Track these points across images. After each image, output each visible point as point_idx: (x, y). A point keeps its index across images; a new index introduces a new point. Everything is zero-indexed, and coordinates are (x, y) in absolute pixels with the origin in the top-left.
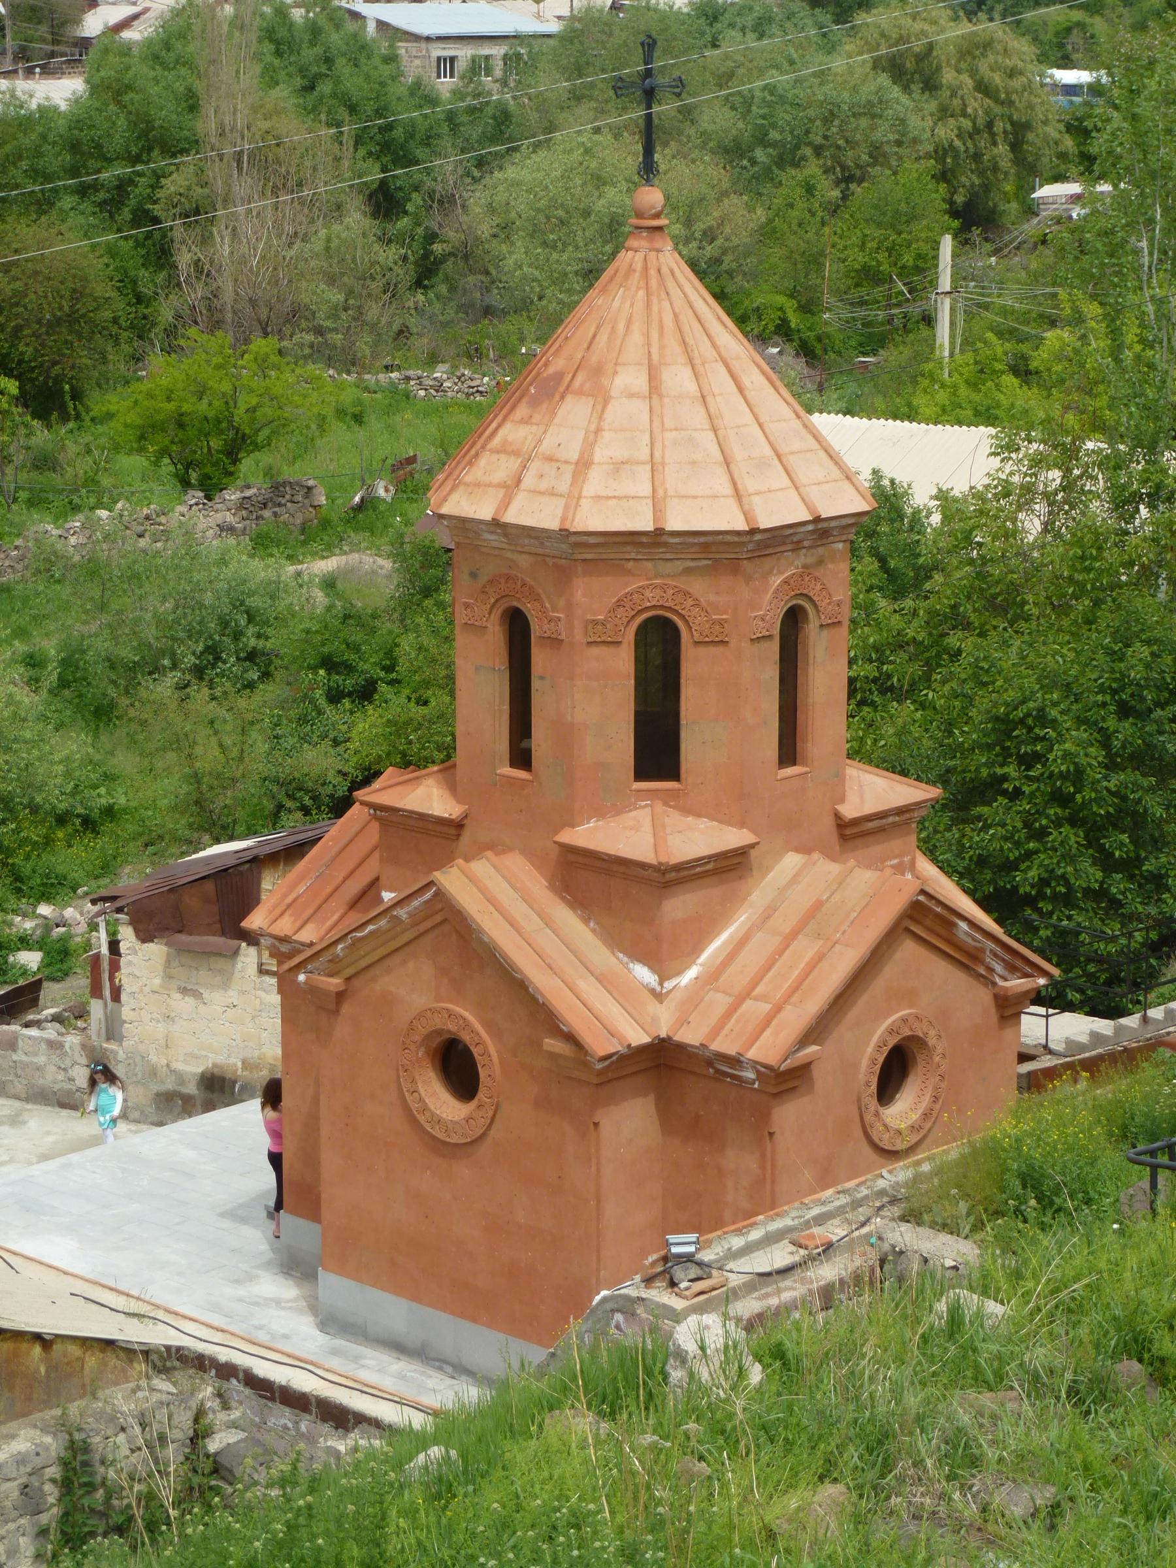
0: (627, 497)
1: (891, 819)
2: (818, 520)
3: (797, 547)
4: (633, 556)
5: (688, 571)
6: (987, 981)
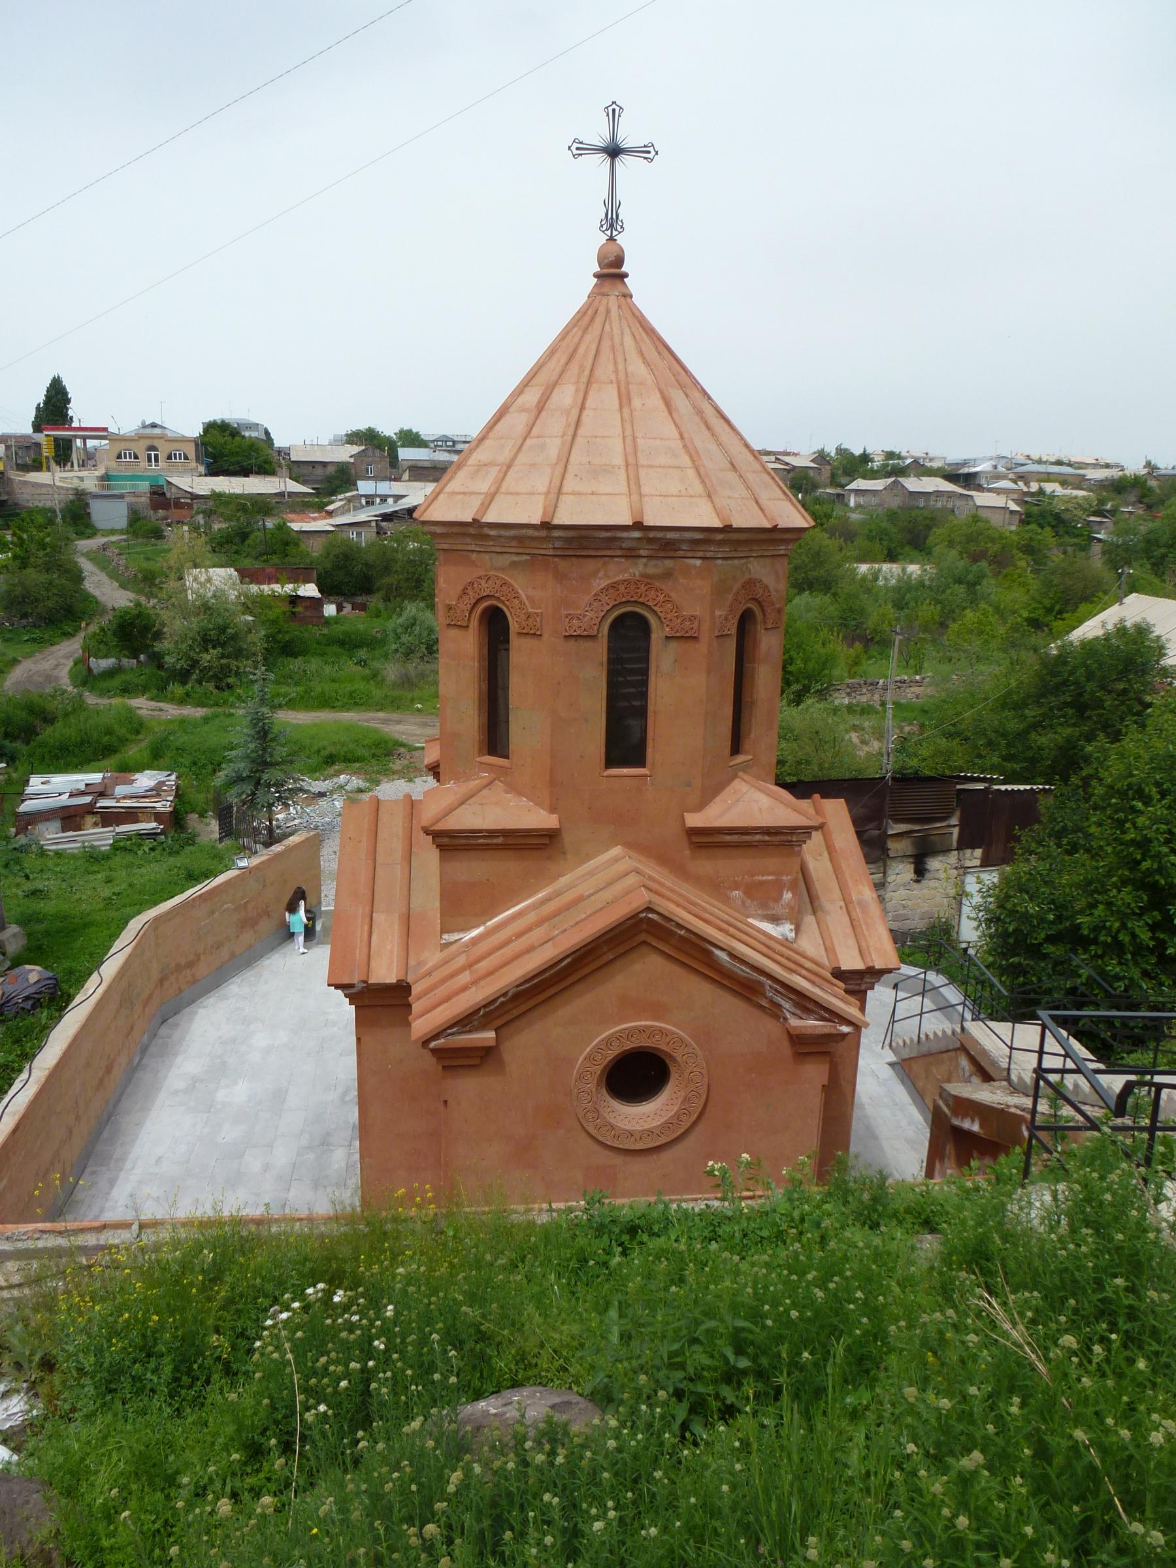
0: (471, 493)
1: (758, 837)
2: (638, 526)
3: (631, 554)
4: (473, 547)
5: (514, 564)
6: (775, 1012)
